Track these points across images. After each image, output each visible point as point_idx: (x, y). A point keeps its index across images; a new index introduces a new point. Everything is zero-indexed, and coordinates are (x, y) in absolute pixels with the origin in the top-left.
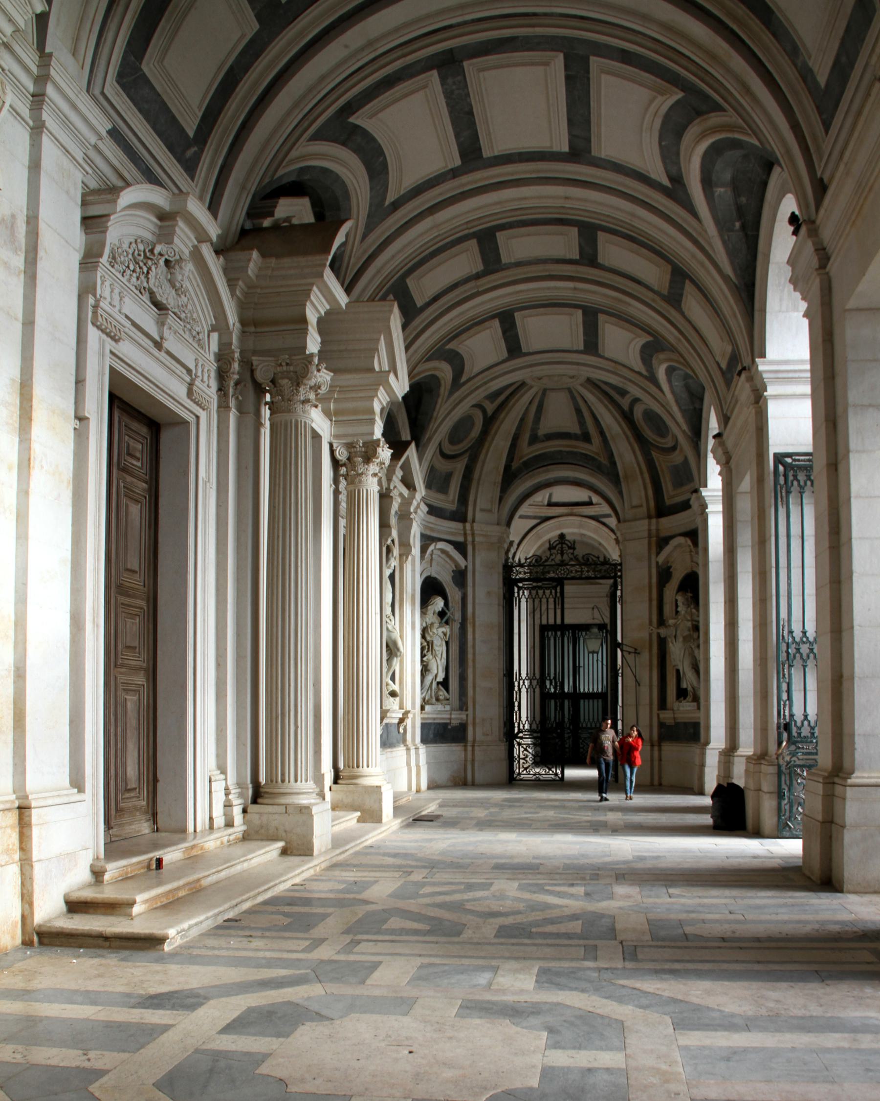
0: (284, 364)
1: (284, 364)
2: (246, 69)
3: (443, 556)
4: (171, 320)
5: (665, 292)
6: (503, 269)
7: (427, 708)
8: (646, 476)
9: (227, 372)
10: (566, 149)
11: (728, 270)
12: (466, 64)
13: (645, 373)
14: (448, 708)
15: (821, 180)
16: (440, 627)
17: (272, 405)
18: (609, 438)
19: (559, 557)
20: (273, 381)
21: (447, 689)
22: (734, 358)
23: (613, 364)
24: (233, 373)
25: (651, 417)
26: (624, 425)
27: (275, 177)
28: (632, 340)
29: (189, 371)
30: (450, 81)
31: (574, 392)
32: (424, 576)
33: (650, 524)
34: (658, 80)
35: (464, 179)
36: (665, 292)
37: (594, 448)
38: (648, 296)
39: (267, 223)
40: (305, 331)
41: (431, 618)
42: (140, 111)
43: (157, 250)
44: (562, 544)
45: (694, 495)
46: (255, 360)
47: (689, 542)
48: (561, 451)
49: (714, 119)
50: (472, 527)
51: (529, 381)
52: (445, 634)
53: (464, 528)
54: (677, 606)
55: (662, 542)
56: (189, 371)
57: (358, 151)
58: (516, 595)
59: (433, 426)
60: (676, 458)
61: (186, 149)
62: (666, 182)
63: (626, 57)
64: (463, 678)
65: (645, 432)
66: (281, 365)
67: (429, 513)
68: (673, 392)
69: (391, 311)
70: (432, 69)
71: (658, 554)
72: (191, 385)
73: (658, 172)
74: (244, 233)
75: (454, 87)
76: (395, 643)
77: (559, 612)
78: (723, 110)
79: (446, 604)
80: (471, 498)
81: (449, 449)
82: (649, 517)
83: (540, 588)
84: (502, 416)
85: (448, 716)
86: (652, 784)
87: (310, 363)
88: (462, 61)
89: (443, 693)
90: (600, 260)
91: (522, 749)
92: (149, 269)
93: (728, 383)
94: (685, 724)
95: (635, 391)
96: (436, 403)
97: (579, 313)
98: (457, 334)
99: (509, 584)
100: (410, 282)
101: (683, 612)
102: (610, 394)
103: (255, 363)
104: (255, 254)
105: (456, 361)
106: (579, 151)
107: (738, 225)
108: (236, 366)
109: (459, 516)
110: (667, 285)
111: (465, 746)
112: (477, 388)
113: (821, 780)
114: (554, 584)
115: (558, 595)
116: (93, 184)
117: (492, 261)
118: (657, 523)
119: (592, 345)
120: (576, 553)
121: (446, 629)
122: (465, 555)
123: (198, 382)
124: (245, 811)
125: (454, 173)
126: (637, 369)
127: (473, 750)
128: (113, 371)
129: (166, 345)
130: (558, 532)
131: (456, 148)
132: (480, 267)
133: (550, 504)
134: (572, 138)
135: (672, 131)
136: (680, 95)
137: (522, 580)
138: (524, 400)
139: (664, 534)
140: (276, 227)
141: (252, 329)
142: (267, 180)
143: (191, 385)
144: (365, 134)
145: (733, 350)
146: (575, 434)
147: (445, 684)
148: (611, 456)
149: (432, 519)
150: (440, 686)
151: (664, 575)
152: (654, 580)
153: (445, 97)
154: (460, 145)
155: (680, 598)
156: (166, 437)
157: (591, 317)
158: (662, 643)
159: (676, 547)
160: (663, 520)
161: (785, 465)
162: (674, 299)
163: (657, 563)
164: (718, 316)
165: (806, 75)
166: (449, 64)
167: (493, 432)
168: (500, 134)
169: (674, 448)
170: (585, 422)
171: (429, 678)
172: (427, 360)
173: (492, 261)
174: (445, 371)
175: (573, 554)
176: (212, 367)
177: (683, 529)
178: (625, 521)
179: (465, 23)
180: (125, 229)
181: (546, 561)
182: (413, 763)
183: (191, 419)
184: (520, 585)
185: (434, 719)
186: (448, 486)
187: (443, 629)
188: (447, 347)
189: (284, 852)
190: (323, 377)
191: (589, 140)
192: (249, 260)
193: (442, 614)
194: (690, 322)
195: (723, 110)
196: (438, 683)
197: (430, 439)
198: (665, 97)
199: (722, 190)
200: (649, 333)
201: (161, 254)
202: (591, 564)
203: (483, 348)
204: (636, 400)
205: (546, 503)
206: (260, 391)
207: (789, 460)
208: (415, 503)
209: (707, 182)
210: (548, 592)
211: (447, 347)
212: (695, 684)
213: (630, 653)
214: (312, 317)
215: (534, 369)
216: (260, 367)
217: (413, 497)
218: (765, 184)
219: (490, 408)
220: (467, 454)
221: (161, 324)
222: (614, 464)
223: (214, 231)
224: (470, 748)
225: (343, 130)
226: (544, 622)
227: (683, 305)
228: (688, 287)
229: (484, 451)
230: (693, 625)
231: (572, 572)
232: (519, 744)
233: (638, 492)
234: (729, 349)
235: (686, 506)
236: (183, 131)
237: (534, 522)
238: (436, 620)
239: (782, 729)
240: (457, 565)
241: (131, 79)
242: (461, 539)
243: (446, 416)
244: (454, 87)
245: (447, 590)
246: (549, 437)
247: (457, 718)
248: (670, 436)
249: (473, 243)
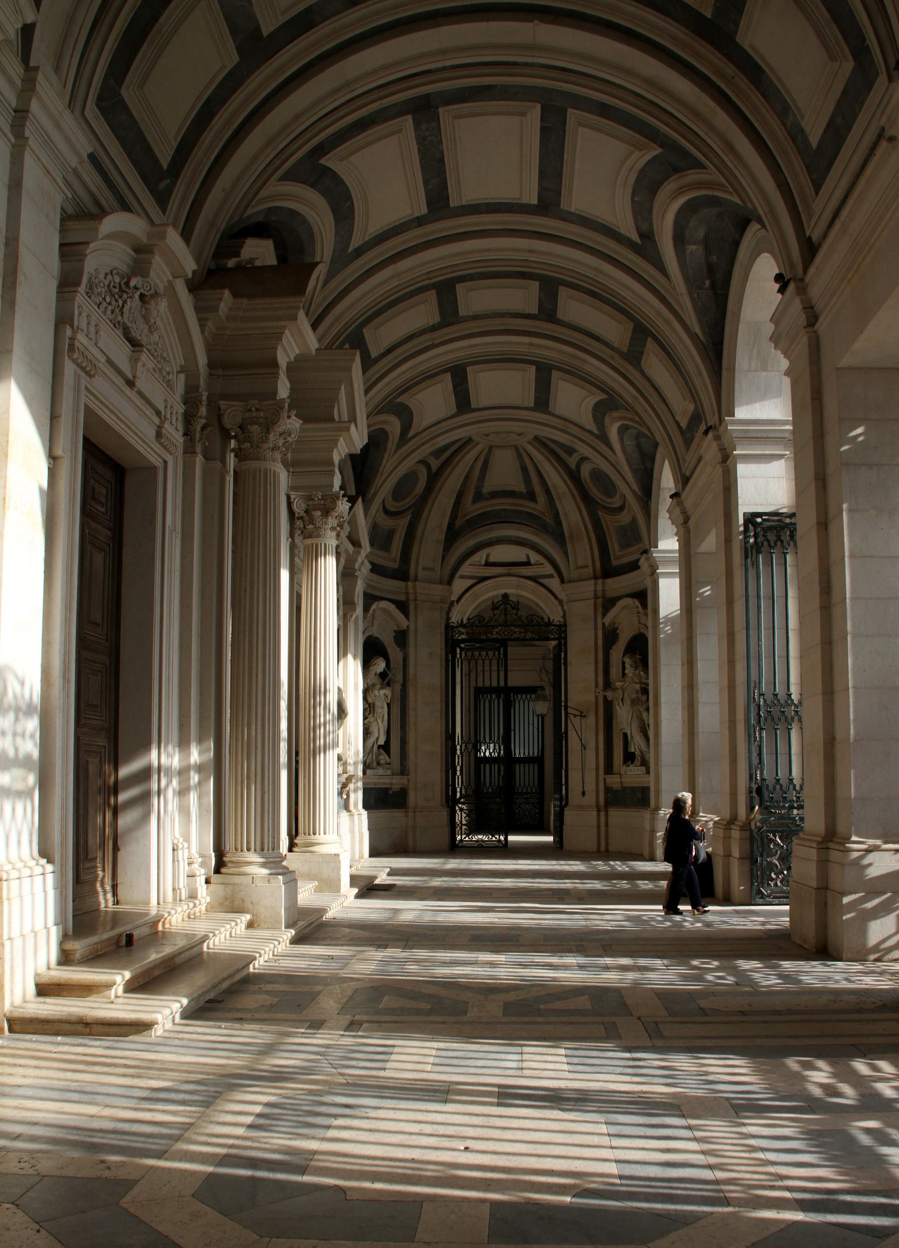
0: (254, 409)
1: (254, 409)
2: (223, 103)
4: (144, 357)
5: (625, 350)
6: (461, 322)
7: (368, 771)
8: (593, 536)
9: (194, 416)
10: (534, 201)
11: (697, 330)
12: (441, 110)
13: (595, 431)
15: (810, 238)
16: (382, 688)
17: (240, 455)
18: (555, 497)
19: (502, 618)
20: (241, 427)
21: (388, 753)
22: (696, 418)
23: (563, 422)
24: (200, 417)
25: (599, 476)
26: (569, 482)
27: (244, 216)
28: (586, 397)
29: (158, 413)
30: (424, 127)
31: (521, 450)
32: (367, 635)
33: (596, 584)
34: (638, 136)
35: (429, 228)
36: (625, 350)
37: (540, 506)
38: (605, 353)
39: (231, 263)
40: (276, 376)
41: (373, 679)
42: (118, 138)
43: (133, 283)
44: (506, 604)
45: (644, 556)
46: (223, 404)
47: (637, 603)
48: (505, 510)
49: (692, 176)
50: (415, 587)
51: (475, 438)
52: (386, 697)
54: (624, 668)
55: (608, 603)
56: (158, 413)
57: (326, 193)
58: (458, 656)
59: (378, 481)
60: (624, 518)
61: (160, 180)
62: (635, 238)
63: (604, 111)
64: (403, 742)
65: (592, 493)
66: (250, 410)
67: (372, 571)
68: (624, 450)
69: (353, 360)
70: (406, 113)
71: (604, 615)
72: (160, 427)
73: (627, 227)
74: (210, 273)
75: (427, 134)
77: (502, 674)
78: (703, 167)
79: (388, 665)
80: (414, 556)
81: (392, 506)
82: (596, 578)
83: (483, 649)
84: (446, 474)
85: (389, 781)
86: (599, 851)
87: (282, 408)
88: (438, 108)
89: (384, 758)
90: (560, 315)
91: (464, 815)
92: (125, 302)
93: (688, 443)
94: (633, 789)
95: (584, 450)
96: (383, 457)
97: (533, 369)
98: (408, 387)
99: (451, 645)
100: (367, 332)
101: (631, 675)
102: (556, 452)
103: (223, 407)
104: (227, 293)
105: (405, 415)
106: (548, 203)
107: (707, 283)
108: (203, 410)
109: (402, 574)
110: (628, 342)
112: (423, 444)
113: (815, 845)
114: (498, 645)
115: (502, 656)
116: (70, 210)
117: (449, 314)
118: (604, 584)
119: (542, 401)
120: (520, 613)
121: (387, 691)
122: (407, 615)
123: (167, 425)
124: (207, 882)
125: (420, 221)
126: (588, 428)
127: (414, 817)
128: (88, 410)
129: (138, 383)
130: (503, 591)
131: (424, 196)
132: (437, 319)
133: (488, 564)
134: (542, 190)
135: (646, 188)
136: (659, 150)
137: (463, 641)
138: (470, 456)
139: (610, 594)
140: (240, 268)
141: (220, 372)
142: (236, 218)
143: (160, 427)
144: (335, 176)
145: (696, 408)
146: (521, 493)
147: (386, 748)
148: (557, 515)
149: (375, 577)
150: (381, 751)
151: (611, 636)
152: (600, 642)
153: (418, 143)
154: (427, 193)
155: (628, 661)
156: (131, 481)
157: (544, 373)
158: (609, 706)
159: (623, 608)
160: (609, 581)
161: (756, 525)
162: (634, 356)
163: (604, 624)
164: (681, 373)
165: (797, 134)
166: (424, 109)
167: (437, 488)
168: (470, 183)
169: (621, 508)
170: (531, 481)
171: (371, 741)
172: (377, 414)
173: (449, 314)
174: (394, 425)
175: (517, 614)
176: (180, 409)
177: (629, 590)
178: (570, 581)
179: (444, 69)
180: (104, 257)
181: (489, 621)
182: (356, 830)
183: (158, 463)
184: (463, 646)
185: (375, 784)
188: (398, 400)
189: (250, 925)
190: (293, 423)
191: (559, 193)
192: (221, 299)
193: (383, 675)
194: (649, 380)
195: (703, 167)
196: (379, 747)
197: (375, 495)
198: (643, 152)
199: (694, 247)
200: (603, 391)
201: (136, 288)
203: (433, 403)
204: (584, 459)
205: (483, 563)
206: (226, 435)
207: (759, 520)
208: (360, 560)
209: (679, 239)
210: (491, 653)
211: (398, 400)
212: (644, 748)
213: (575, 716)
214: (283, 361)
215: (483, 425)
216: (228, 411)
217: (359, 553)
218: (737, 244)
219: (435, 464)
220: (410, 511)
221: (134, 361)
222: (559, 523)
223: (190, 266)
225: (314, 172)
226: (480, 684)
227: (643, 363)
228: (650, 344)
230: (641, 688)
231: (515, 633)
232: (461, 810)
233: (583, 553)
234: (691, 407)
235: (634, 566)
236: (156, 161)
237: (471, 582)
238: (377, 681)
239: (754, 794)
241: (111, 105)
242: (402, 598)
243: (392, 470)
244: (427, 134)
246: (494, 495)
247: (396, 783)
248: (618, 496)
249: (434, 292)
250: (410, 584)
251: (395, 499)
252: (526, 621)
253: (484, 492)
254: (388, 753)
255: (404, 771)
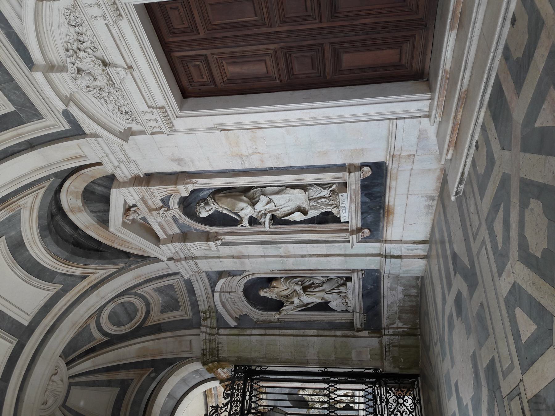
55: (221, 324)
175: (221, 408)
202: (232, 393)
231: (236, 410)
252: (229, 399)
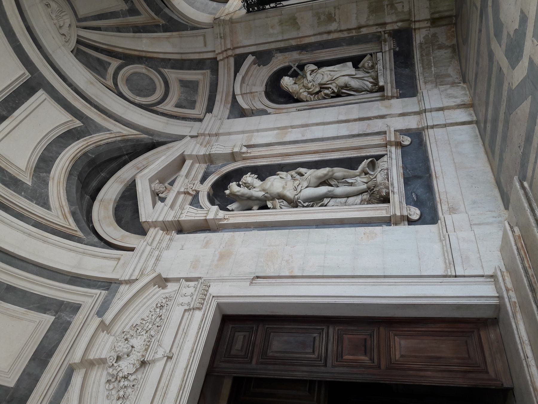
3: (247, 79)
7: (381, 83)
14: (379, 55)
16: (306, 77)
21: (361, 58)
50: (222, 53)
51: (73, 43)
53: (223, 60)
76: (319, 178)
80: (196, 57)
84: (120, 50)
89: (366, 62)
111: (415, 29)
127: (419, 21)
147: (356, 62)
150: (360, 66)
171: (354, 83)
185: (391, 70)
186: (191, 82)
187: (308, 74)
193: (295, 75)
219: (115, 63)
220: (163, 70)
224: (417, 25)
229: (155, 55)
240: (254, 63)
242: (232, 60)
245: (275, 69)
250: (219, 57)
251: (154, 91)
253: (127, 8)
254: (361, 58)
255: (377, 39)
